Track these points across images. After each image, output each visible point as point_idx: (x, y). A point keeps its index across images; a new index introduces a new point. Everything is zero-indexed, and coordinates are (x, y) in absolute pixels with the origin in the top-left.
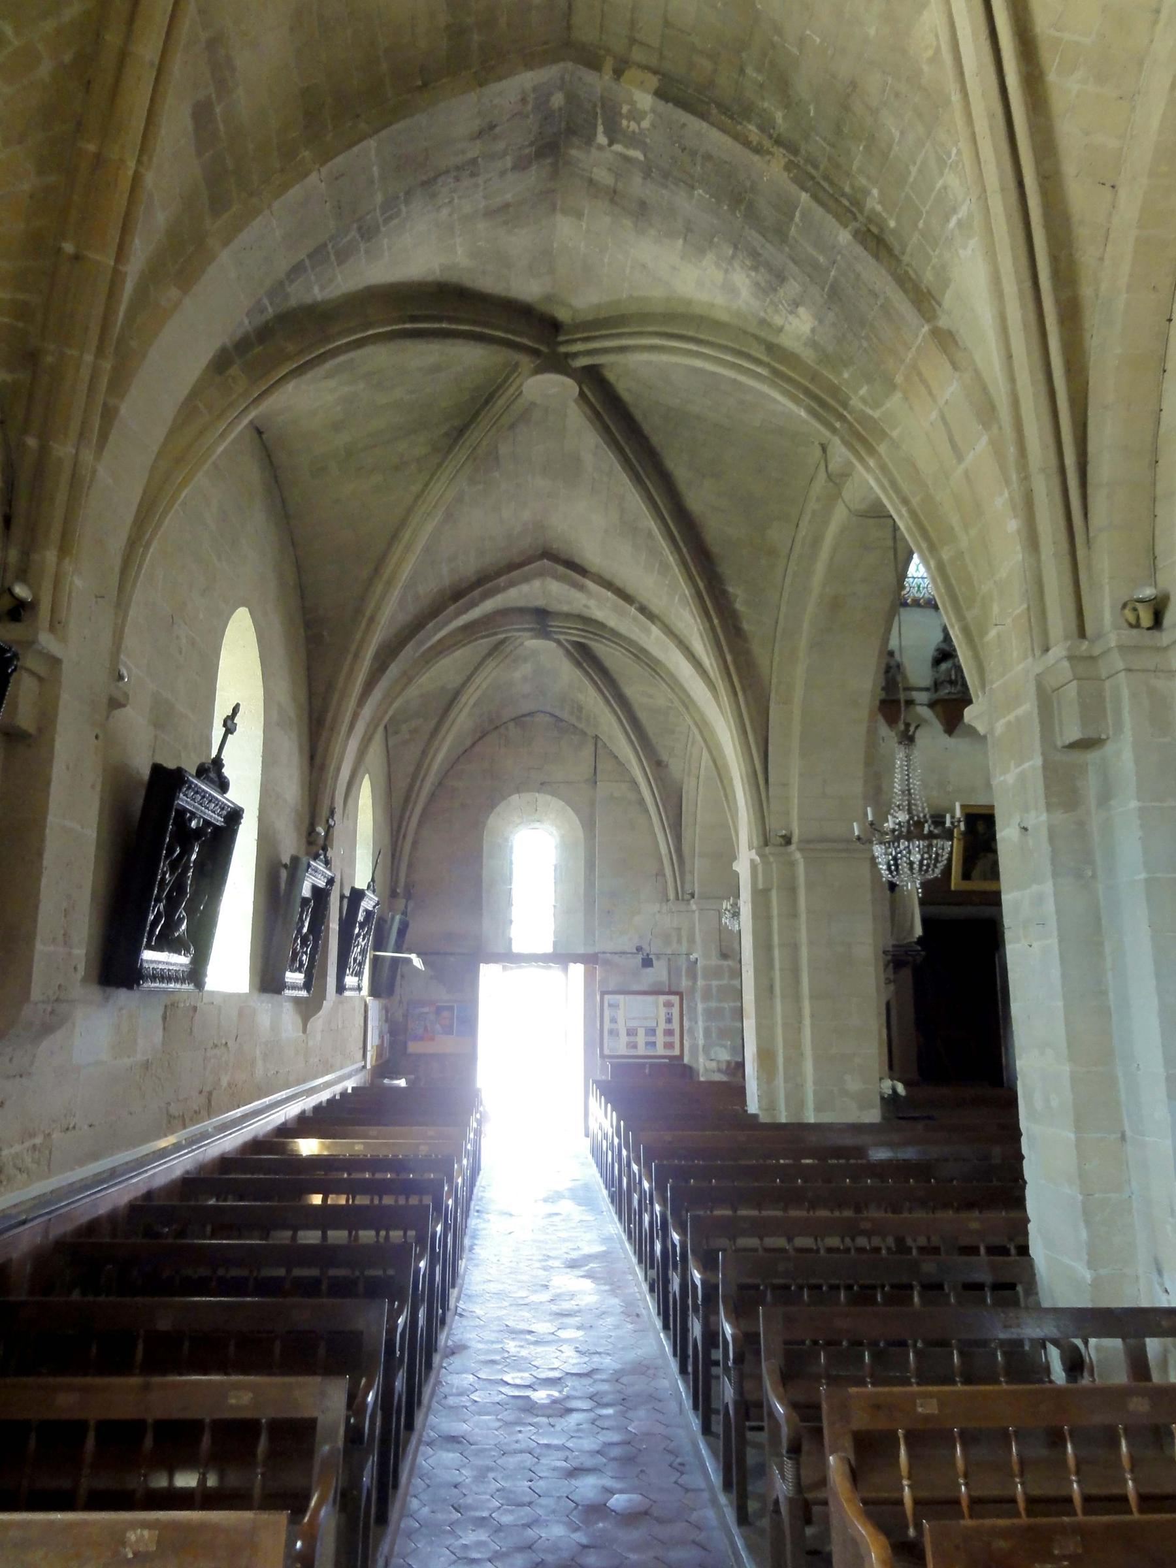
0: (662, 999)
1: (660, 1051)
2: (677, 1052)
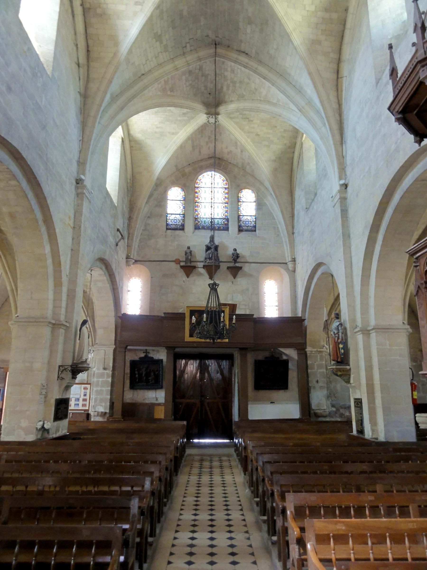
0: (83, 386)
1: (80, 407)
2: (87, 408)
